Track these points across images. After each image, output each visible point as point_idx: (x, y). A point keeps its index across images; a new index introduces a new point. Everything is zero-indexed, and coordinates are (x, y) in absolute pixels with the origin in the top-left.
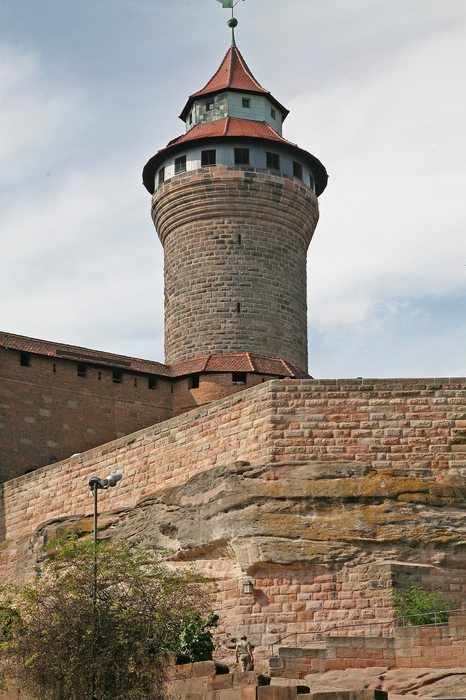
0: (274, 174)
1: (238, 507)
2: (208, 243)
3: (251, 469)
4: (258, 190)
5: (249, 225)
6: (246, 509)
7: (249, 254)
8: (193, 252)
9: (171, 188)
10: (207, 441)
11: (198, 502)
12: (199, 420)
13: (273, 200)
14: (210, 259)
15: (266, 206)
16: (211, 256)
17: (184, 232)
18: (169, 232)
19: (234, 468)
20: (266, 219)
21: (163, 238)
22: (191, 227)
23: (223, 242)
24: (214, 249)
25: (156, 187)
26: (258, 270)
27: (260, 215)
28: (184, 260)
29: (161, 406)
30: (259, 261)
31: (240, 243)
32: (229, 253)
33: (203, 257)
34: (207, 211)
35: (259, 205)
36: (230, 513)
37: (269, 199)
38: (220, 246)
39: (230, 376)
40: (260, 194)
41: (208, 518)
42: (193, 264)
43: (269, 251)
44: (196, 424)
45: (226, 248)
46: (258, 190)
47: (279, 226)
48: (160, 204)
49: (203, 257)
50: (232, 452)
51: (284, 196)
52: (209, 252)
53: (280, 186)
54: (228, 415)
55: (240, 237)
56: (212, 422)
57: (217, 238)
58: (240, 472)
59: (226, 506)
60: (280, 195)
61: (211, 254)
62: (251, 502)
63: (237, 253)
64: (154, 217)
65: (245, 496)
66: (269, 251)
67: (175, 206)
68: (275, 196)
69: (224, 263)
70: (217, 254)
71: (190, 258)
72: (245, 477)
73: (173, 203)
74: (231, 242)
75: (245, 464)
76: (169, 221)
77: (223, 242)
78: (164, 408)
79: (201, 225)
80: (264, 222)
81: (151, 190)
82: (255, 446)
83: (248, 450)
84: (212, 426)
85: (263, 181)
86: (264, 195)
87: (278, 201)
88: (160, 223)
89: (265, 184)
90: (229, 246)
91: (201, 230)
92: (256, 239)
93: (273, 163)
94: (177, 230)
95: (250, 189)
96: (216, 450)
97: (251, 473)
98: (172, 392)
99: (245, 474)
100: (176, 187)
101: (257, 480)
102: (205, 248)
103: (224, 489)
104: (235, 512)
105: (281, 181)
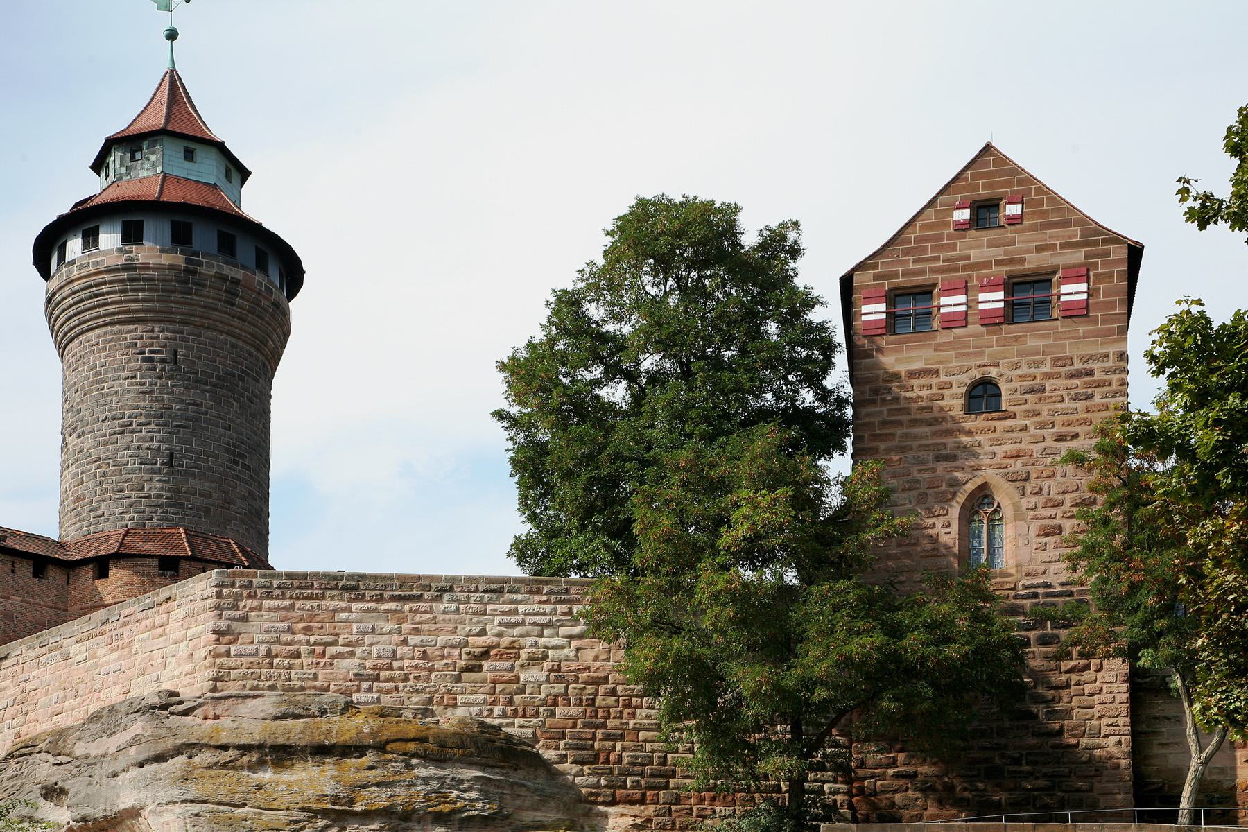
1: (159, 758)
3: (181, 703)
4: (204, 286)
6: (170, 761)
9: (76, 273)
10: (118, 659)
11: (101, 752)
12: (105, 627)
13: (225, 302)
15: (216, 310)
17: (93, 342)
18: (72, 340)
19: (157, 701)
21: (62, 348)
22: (105, 334)
25: (53, 270)
26: (201, 405)
30: (204, 391)
31: (176, 363)
32: (160, 377)
34: (128, 312)
35: (205, 307)
36: (146, 767)
37: (219, 300)
38: (146, 365)
40: (207, 291)
41: (115, 775)
43: (218, 378)
44: (102, 633)
46: (204, 286)
47: (233, 340)
48: (58, 297)
50: (154, 675)
54: (151, 620)
55: (176, 353)
56: (126, 630)
57: (143, 353)
58: (164, 707)
59: (141, 757)
60: (237, 295)
62: (178, 751)
63: (171, 377)
64: (49, 316)
65: (170, 743)
66: (218, 378)
67: (82, 301)
70: (142, 377)
72: (172, 714)
73: (77, 297)
74: (163, 361)
75: (173, 694)
76: (72, 323)
77: (151, 360)
79: (119, 332)
80: (212, 334)
81: (46, 274)
82: (188, 667)
83: (177, 673)
84: (125, 636)
86: (212, 293)
87: (233, 305)
88: (57, 326)
90: (160, 366)
91: (119, 339)
92: (199, 358)
94: (82, 338)
95: (193, 283)
96: (130, 673)
97: (180, 708)
99: (171, 709)
100: (83, 272)
101: (188, 719)
103: (139, 731)
104: (154, 766)
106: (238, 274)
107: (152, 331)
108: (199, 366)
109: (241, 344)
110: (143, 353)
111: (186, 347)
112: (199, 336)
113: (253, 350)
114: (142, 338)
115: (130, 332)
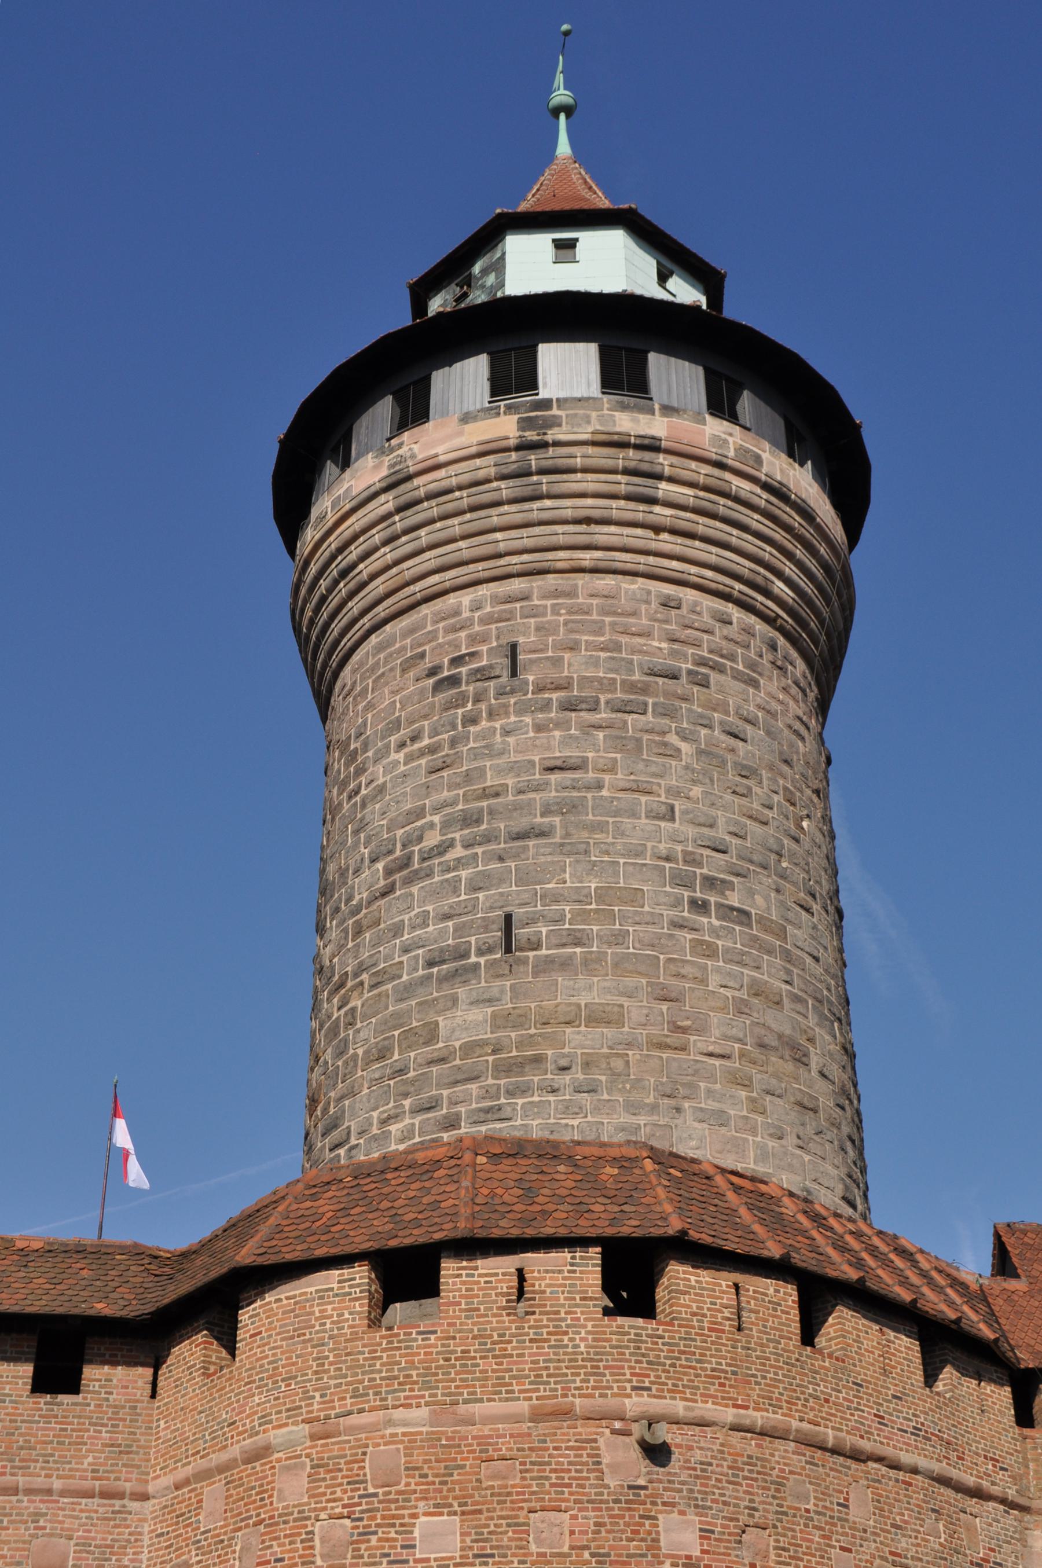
5: (549, 603)
7: (546, 706)
8: (365, 748)
14: (410, 758)
16: (417, 746)
20: (615, 572)
23: (454, 681)
24: (425, 717)
27: (587, 558)
29: (87, 1484)
39: (361, 1274)
42: (363, 792)
45: (461, 700)
49: (393, 756)
51: (671, 480)
52: (404, 732)
53: (652, 446)
61: (414, 739)
71: (360, 771)
74: (483, 675)
77: (454, 681)
78: (105, 1495)
87: (652, 501)
91: (386, 662)
92: (573, 647)
93: (623, 377)
102: (398, 719)
105: (657, 426)
107: (457, 613)
108: (574, 666)
109: (689, 595)
110: (433, 672)
112: (571, 594)
113: (731, 609)
115: (411, 631)
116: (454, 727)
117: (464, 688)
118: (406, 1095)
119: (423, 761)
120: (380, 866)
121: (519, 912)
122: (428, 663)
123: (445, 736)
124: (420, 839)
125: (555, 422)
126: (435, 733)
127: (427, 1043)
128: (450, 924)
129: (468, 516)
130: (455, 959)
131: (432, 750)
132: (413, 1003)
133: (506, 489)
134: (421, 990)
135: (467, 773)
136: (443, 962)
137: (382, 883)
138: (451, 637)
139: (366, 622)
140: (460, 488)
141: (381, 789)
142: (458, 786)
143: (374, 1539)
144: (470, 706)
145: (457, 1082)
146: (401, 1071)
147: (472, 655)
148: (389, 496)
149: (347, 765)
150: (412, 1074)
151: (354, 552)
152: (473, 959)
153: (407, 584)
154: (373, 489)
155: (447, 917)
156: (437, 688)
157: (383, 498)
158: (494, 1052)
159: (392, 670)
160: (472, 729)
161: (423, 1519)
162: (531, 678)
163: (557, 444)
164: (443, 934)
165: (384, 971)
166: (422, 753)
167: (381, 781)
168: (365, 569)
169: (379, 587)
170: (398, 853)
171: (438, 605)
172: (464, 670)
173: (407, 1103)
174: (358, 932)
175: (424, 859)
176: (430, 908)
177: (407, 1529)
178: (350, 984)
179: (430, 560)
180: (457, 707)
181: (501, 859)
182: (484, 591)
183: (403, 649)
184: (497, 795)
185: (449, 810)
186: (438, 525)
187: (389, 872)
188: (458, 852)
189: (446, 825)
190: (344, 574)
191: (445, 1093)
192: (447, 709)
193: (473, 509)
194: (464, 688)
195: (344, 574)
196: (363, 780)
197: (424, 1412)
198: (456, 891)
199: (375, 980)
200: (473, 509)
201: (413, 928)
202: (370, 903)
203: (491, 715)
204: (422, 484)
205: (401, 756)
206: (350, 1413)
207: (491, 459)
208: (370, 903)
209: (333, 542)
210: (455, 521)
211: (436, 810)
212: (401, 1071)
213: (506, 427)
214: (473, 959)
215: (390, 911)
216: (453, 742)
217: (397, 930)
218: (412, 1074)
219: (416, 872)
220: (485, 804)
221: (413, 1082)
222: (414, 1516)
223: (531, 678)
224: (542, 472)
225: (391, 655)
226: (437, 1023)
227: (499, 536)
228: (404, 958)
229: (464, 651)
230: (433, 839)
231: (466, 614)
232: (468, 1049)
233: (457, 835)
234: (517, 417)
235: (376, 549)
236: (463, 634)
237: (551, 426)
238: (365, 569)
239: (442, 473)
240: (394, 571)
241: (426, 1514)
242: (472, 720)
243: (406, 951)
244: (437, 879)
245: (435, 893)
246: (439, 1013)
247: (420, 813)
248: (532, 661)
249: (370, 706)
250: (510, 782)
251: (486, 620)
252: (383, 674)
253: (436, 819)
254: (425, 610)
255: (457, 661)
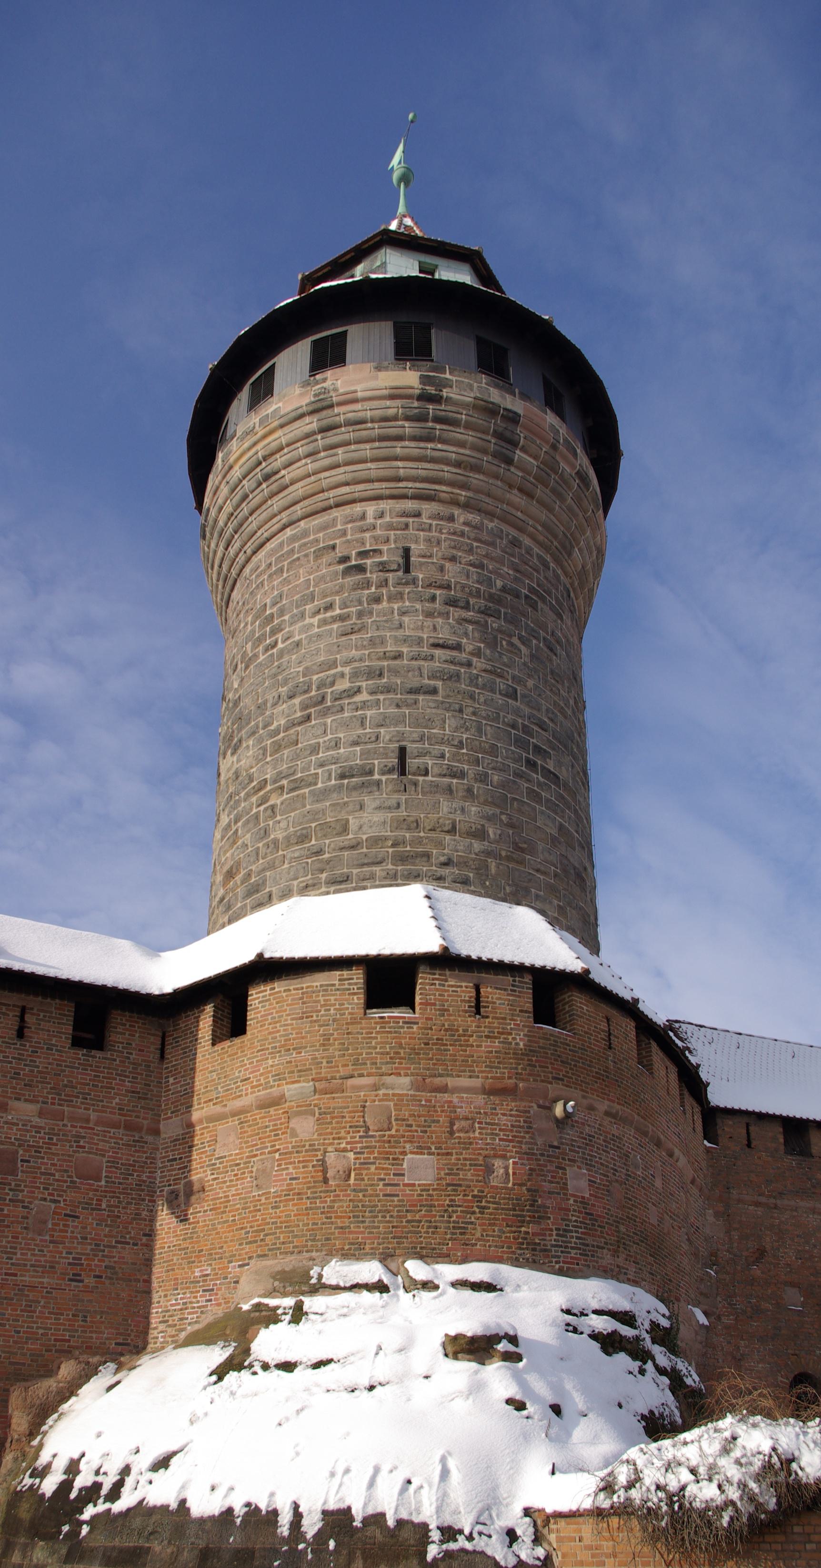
0: (496, 386)
2: (322, 579)
5: (434, 523)
8: (282, 612)
14: (324, 622)
16: (329, 614)
23: (361, 569)
24: (337, 593)
28: (260, 640)
31: (407, 570)
33: (308, 621)
38: (350, 580)
42: (280, 645)
45: (368, 584)
49: (308, 621)
63: (400, 596)
68: (503, 444)
69: (362, 628)
74: (383, 567)
77: (361, 569)
85: (468, 398)
86: (470, 437)
89: (475, 407)
90: (374, 577)
92: (453, 559)
94: (247, 570)
98: (162, 1057)
106: (517, 405)
107: (363, 517)
110: (345, 559)
111: (428, 540)
114: (344, 533)
115: (324, 528)
116: (360, 603)
117: (368, 575)
118: (322, 871)
119: (335, 626)
120: (297, 701)
121: (411, 747)
122: (339, 553)
123: (354, 609)
124: (333, 684)
125: (447, 384)
126: (344, 606)
127: (339, 834)
128: (358, 749)
129: (377, 444)
130: (362, 775)
131: (342, 618)
132: (328, 804)
133: (408, 428)
134: (335, 795)
135: (371, 639)
136: (352, 776)
137: (299, 714)
138: (358, 536)
139: (284, 517)
140: (372, 421)
141: (298, 644)
142: (364, 647)
143: (373, 1167)
144: (373, 589)
145: (363, 865)
146: (319, 852)
147: (374, 551)
148: (315, 418)
149: (262, 626)
150: (327, 856)
151: (279, 461)
152: (376, 776)
153: (323, 491)
154: (300, 411)
155: (356, 743)
156: (347, 572)
157: (307, 419)
158: (393, 846)
159: (306, 556)
160: (375, 606)
161: (410, 1156)
162: (421, 576)
163: (448, 400)
164: (355, 756)
165: (302, 780)
166: (334, 619)
167: (297, 638)
168: (287, 475)
169: (298, 490)
170: (313, 693)
171: (347, 510)
172: (369, 562)
173: (324, 876)
174: (278, 747)
175: (336, 699)
176: (341, 735)
177: (397, 1162)
178: (269, 788)
179: (340, 474)
180: (363, 589)
181: (398, 706)
182: (384, 505)
183: (317, 541)
184: (395, 658)
185: (356, 664)
186: (353, 447)
187: (304, 707)
188: (364, 696)
189: (355, 675)
190: (267, 478)
191: (355, 871)
192: (355, 589)
193: (382, 438)
194: (368, 575)
195: (267, 478)
196: (280, 636)
197: (406, 1081)
198: (362, 724)
199: (292, 785)
200: (382, 438)
201: (328, 749)
202: (287, 729)
203: (390, 599)
204: (342, 413)
205: (315, 620)
206: (352, 1077)
207: (398, 403)
208: (287, 729)
209: (260, 450)
210: (368, 446)
211: (347, 663)
212: (319, 852)
213: (409, 378)
214: (376, 776)
215: (308, 736)
216: (360, 614)
217: (315, 749)
218: (327, 856)
219: (329, 708)
220: (386, 663)
221: (328, 861)
222: (404, 1153)
223: (421, 576)
224: (438, 420)
225: (305, 544)
226: (347, 821)
227: (400, 464)
228: (320, 771)
229: (368, 548)
230: (343, 685)
231: (370, 520)
232: (375, 841)
233: (364, 684)
234: (419, 373)
235: (299, 460)
236: (367, 535)
237: (445, 387)
238: (287, 475)
239: (358, 406)
240: (313, 478)
241: (412, 1153)
242: (377, 600)
243: (322, 765)
244: (346, 715)
245: (346, 725)
246: (349, 813)
247: (334, 664)
248: (421, 564)
249: (287, 581)
250: (405, 650)
251: (390, 527)
252: (298, 559)
253: (347, 670)
254: (336, 513)
255: (363, 554)
